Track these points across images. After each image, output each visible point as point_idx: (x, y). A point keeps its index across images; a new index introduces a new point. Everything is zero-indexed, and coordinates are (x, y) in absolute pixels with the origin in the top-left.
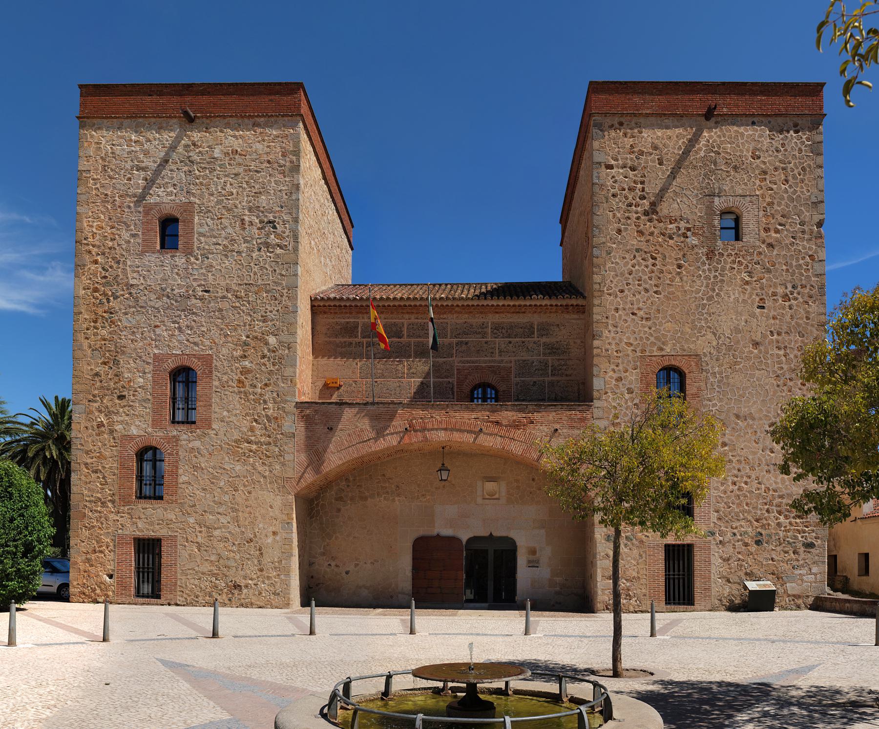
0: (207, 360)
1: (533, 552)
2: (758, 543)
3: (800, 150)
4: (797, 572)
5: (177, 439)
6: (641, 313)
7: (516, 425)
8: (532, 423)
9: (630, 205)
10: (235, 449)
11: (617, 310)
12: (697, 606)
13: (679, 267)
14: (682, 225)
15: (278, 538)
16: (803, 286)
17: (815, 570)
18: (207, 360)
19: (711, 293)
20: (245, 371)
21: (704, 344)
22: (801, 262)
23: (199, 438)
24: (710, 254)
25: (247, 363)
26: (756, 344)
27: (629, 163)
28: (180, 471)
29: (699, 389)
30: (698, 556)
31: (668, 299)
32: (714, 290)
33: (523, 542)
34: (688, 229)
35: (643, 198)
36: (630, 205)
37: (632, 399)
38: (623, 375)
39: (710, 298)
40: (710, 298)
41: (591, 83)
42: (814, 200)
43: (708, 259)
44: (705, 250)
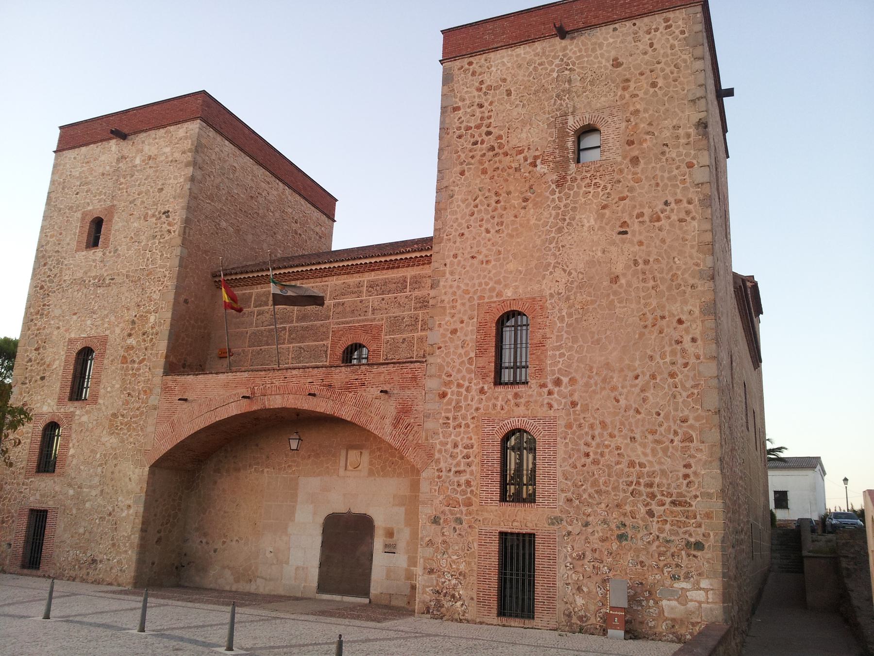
0: (104, 341)
1: (390, 534)
2: (621, 537)
3: (672, 47)
4: (678, 585)
5: (73, 413)
6: (480, 257)
7: (348, 387)
8: (363, 384)
9: (475, 143)
10: (114, 423)
11: (455, 256)
12: (537, 622)
13: (526, 200)
14: (530, 155)
15: (131, 511)
16: (678, 202)
17: (705, 584)
18: (104, 341)
19: (560, 224)
20: (130, 348)
21: (550, 285)
22: (676, 172)
23: (87, 412)
24: (560, 183)
25: (132, 341)
26: (615, 279)
27: (477, 100)
28: (71, 445)
29: (544, 337)
30: (540, 550)
31: (511, 236)
32: (565, 220)
33: (380, 522)
34: (536, 158)
35: (489, 133)
36: (475, 143)
37: (467, 353)
38: (459, 326)
39: (560, 230)
40: (560, 230)
41: (447, 33)
42: (691, 97)
43: (558, 186)
44: (555, 177)
